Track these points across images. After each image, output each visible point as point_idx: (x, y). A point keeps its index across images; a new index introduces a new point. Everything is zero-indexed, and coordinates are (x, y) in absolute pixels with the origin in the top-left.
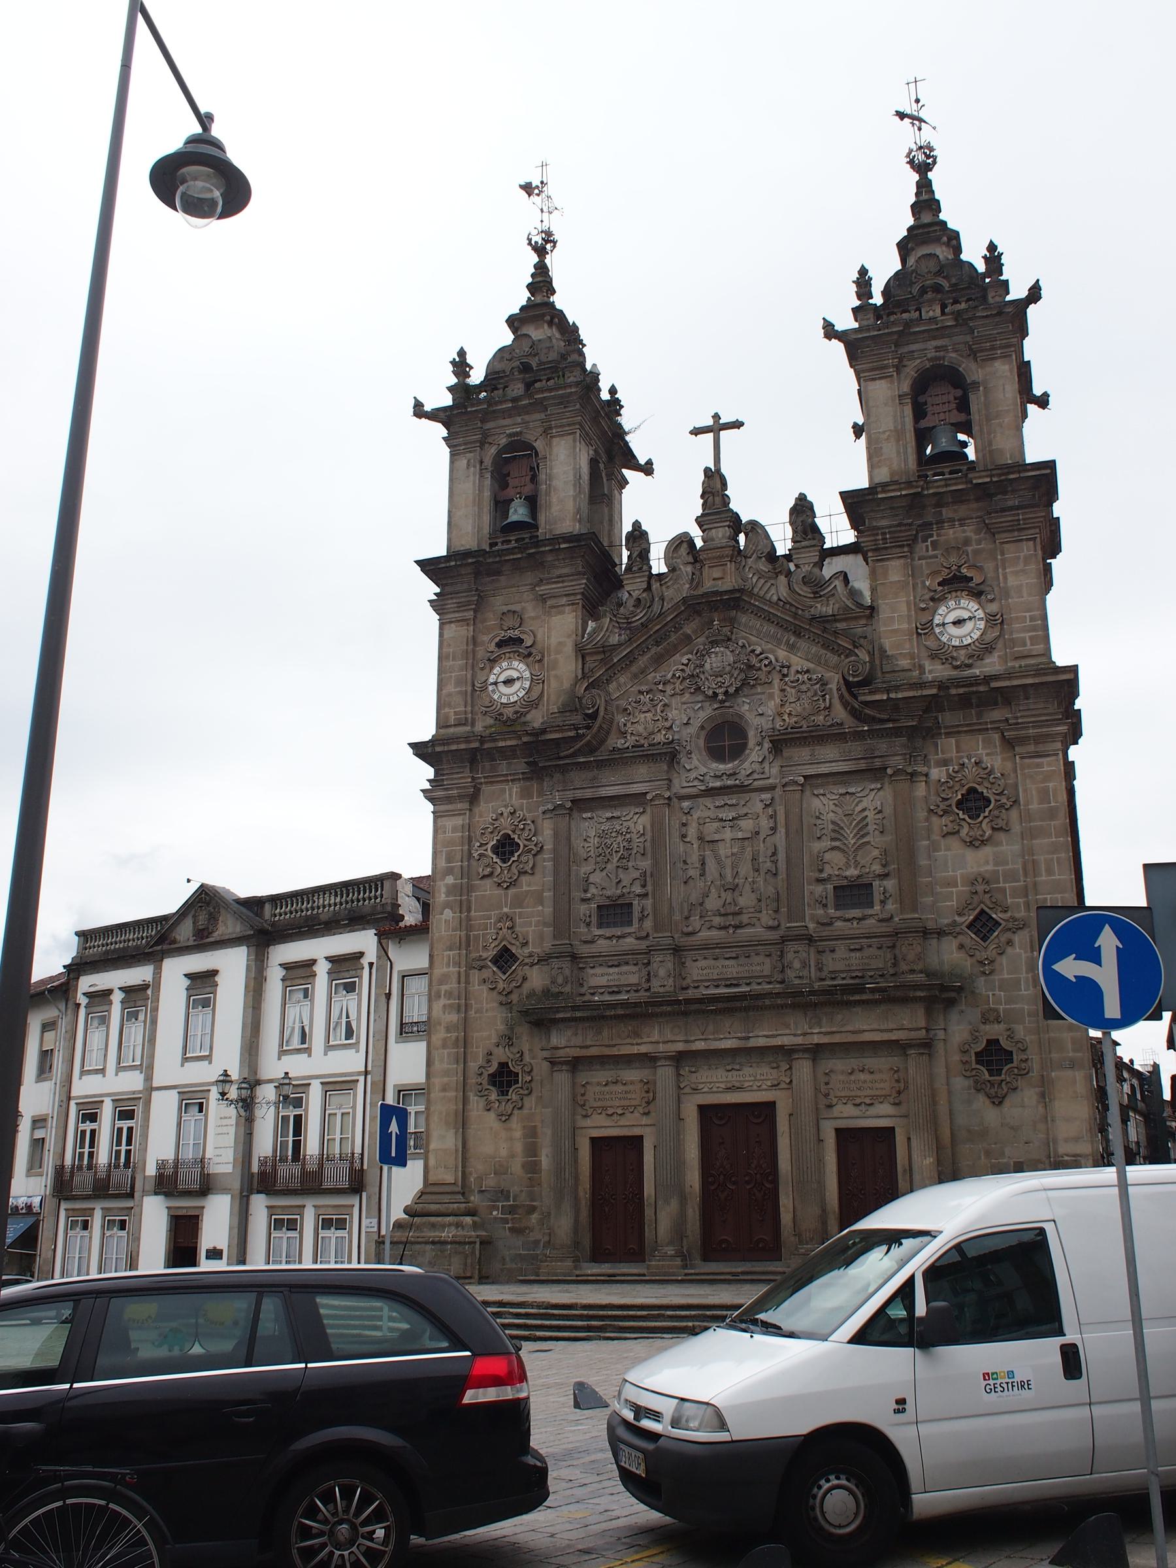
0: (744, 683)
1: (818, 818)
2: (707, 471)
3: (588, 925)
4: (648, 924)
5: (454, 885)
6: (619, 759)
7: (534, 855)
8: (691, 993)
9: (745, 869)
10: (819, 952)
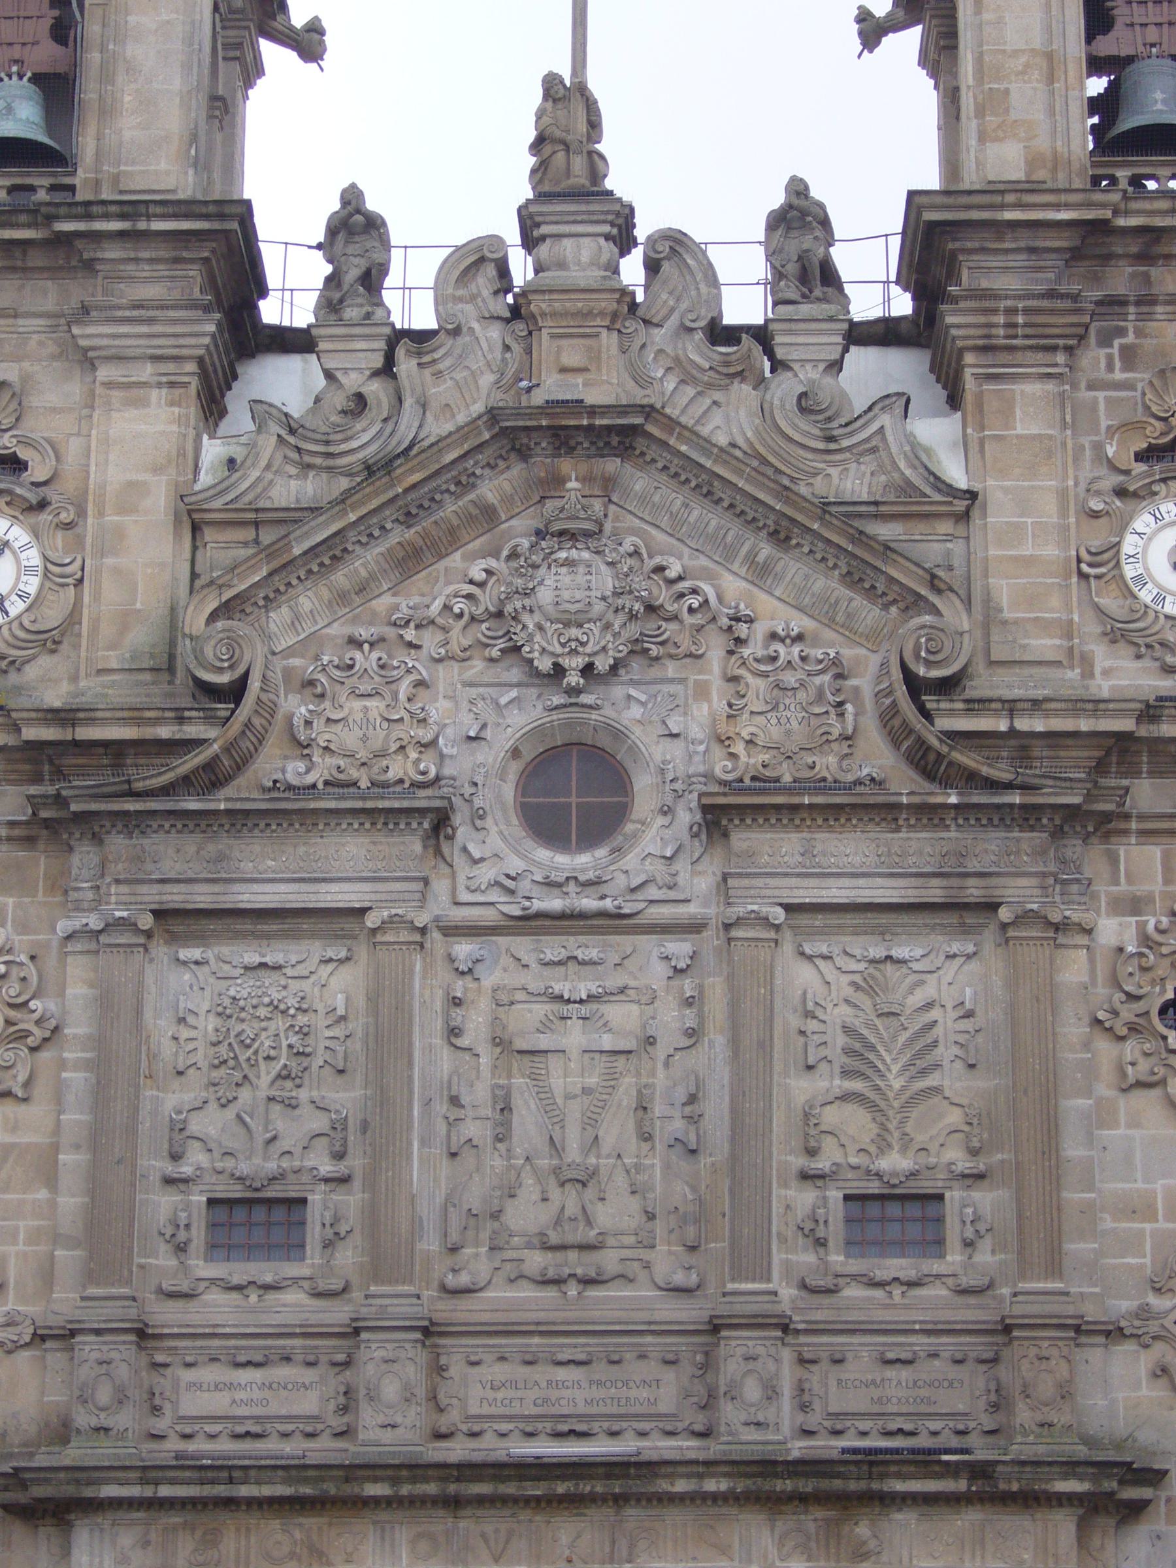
0: (638, 650)
1: (809, 1015)
2: (551, 83)
3: (181, 1249)
4: (347, 1258)
6: (290, 814)
7: (33, 1050)
8: (457, 1451)
9: (617, 1130)
10: (802, 1361)
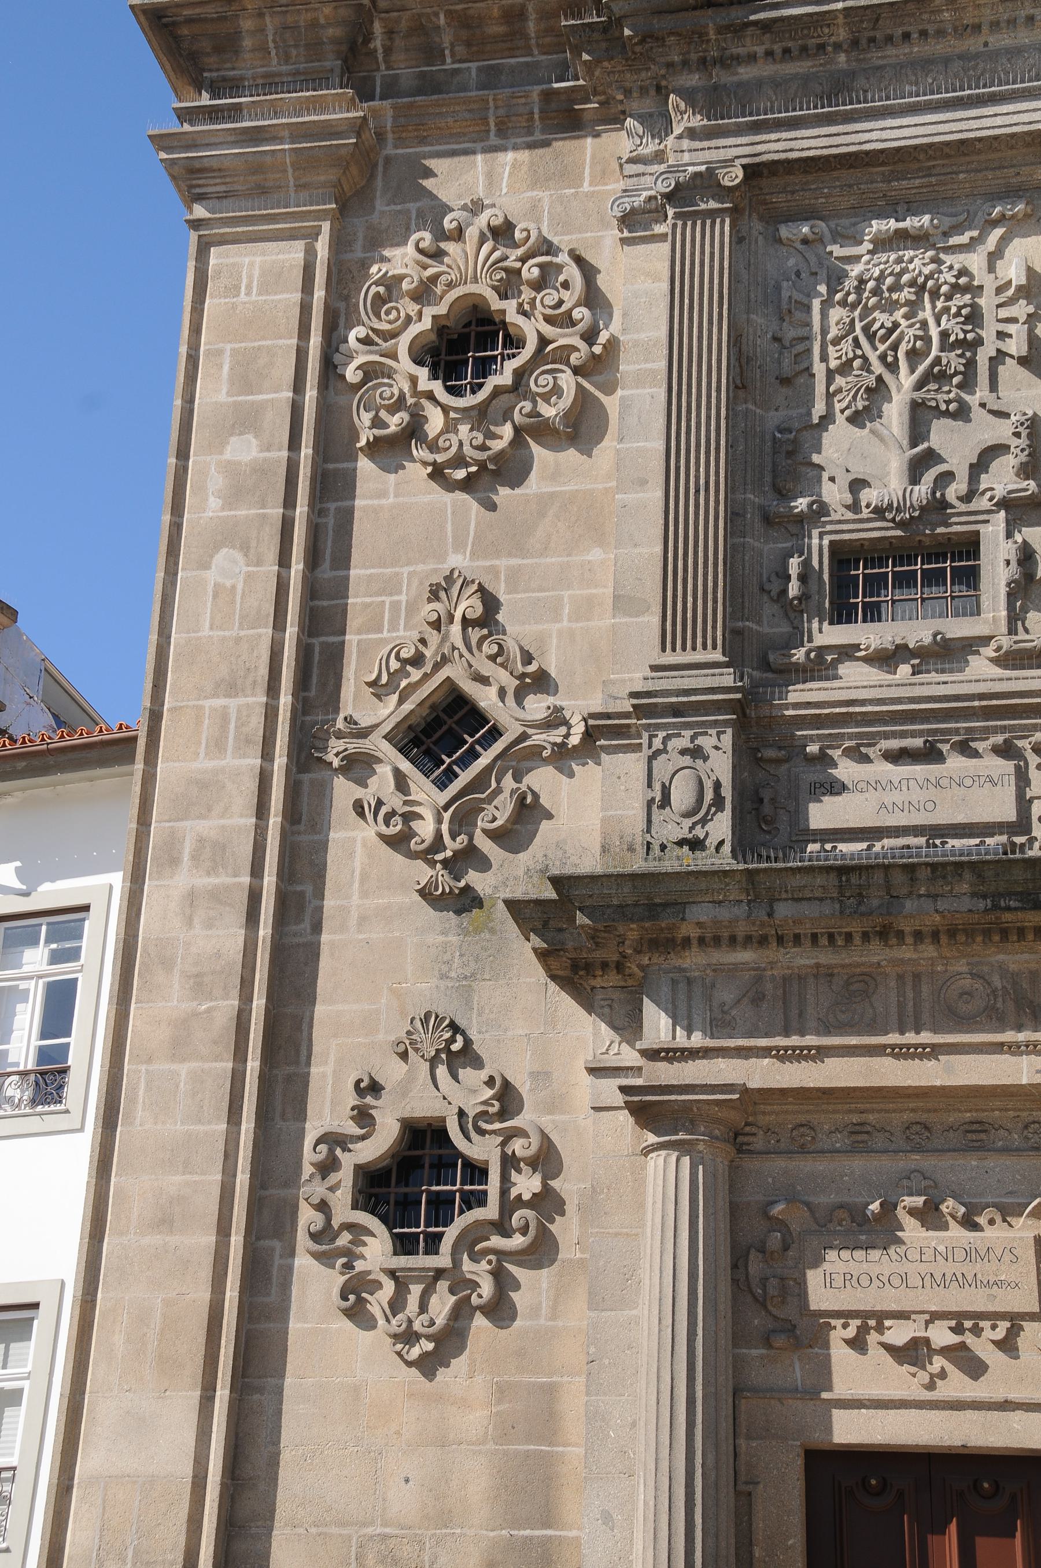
5: (260, 470)
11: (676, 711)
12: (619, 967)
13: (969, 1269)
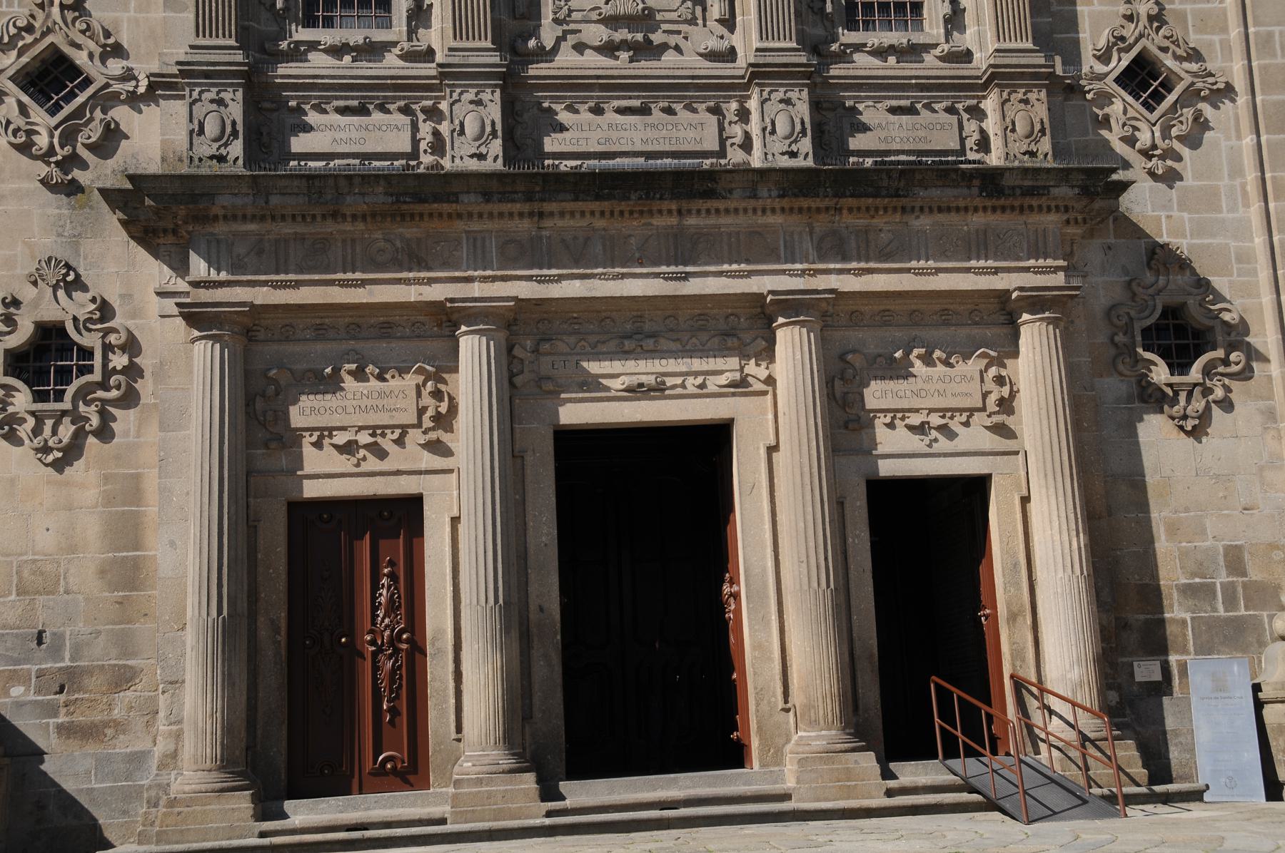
11: (207, 75)
12: (175, 232)
13: (380, 403)
